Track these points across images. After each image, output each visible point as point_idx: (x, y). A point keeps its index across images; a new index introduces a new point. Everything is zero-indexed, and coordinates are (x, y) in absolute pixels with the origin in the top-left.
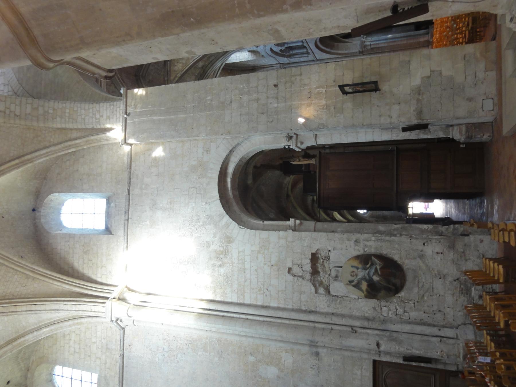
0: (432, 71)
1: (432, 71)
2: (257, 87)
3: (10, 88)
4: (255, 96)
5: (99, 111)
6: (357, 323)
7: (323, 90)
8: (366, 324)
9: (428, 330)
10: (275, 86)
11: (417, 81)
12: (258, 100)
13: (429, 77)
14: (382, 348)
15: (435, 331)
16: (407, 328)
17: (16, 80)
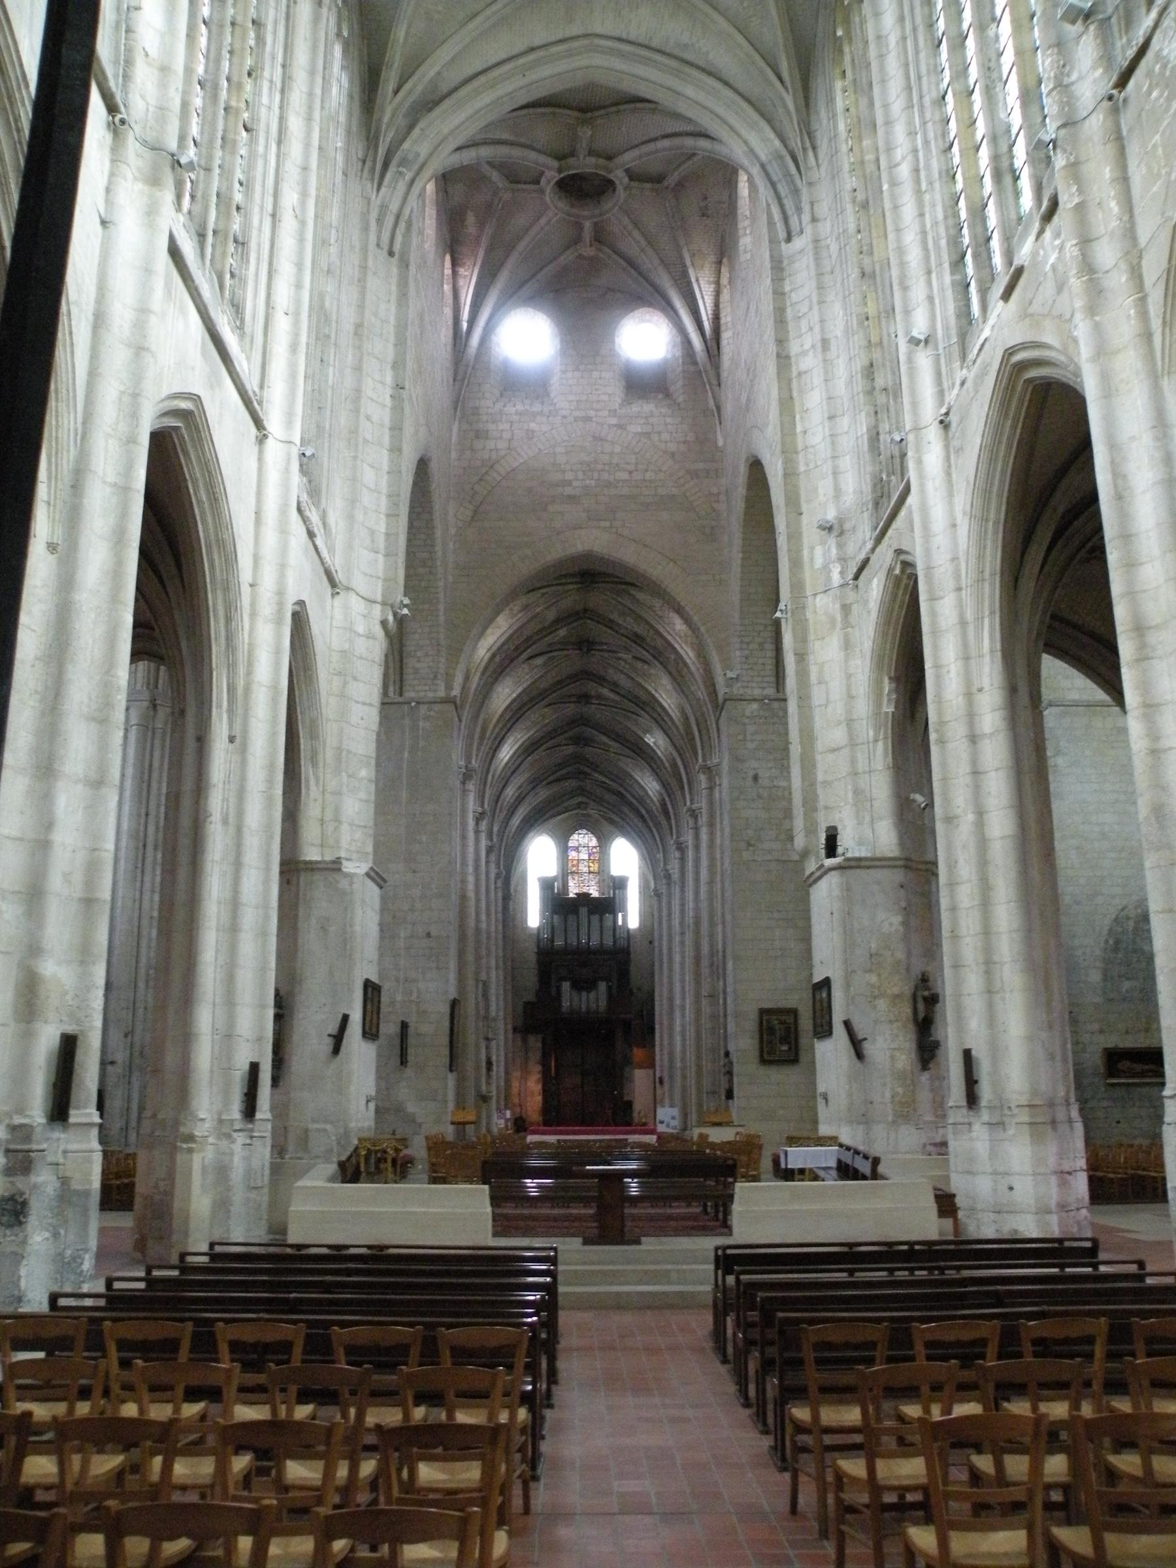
0: (420, 1125)
1: (420, 1125)
2: (430, 909)
3: (503, 453)
4: (418, 905)
5: (427, 655)
6: (137, 1038)
7: (414, 997)
8: (137, 1048)
9: (134, 1115)
10: (429, 935)
11: (411, 1108)
12: (412, 910)
13: (414, 1121)
14: (109, 1068)
15: (133, 1123)
16: (135, 1096)
17: (516, 464)
